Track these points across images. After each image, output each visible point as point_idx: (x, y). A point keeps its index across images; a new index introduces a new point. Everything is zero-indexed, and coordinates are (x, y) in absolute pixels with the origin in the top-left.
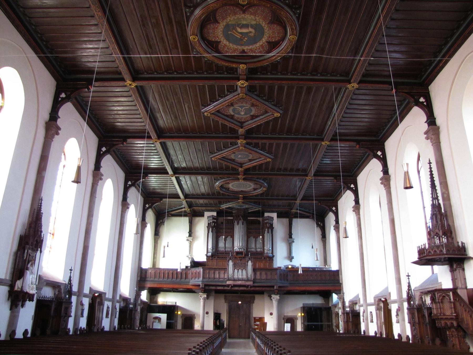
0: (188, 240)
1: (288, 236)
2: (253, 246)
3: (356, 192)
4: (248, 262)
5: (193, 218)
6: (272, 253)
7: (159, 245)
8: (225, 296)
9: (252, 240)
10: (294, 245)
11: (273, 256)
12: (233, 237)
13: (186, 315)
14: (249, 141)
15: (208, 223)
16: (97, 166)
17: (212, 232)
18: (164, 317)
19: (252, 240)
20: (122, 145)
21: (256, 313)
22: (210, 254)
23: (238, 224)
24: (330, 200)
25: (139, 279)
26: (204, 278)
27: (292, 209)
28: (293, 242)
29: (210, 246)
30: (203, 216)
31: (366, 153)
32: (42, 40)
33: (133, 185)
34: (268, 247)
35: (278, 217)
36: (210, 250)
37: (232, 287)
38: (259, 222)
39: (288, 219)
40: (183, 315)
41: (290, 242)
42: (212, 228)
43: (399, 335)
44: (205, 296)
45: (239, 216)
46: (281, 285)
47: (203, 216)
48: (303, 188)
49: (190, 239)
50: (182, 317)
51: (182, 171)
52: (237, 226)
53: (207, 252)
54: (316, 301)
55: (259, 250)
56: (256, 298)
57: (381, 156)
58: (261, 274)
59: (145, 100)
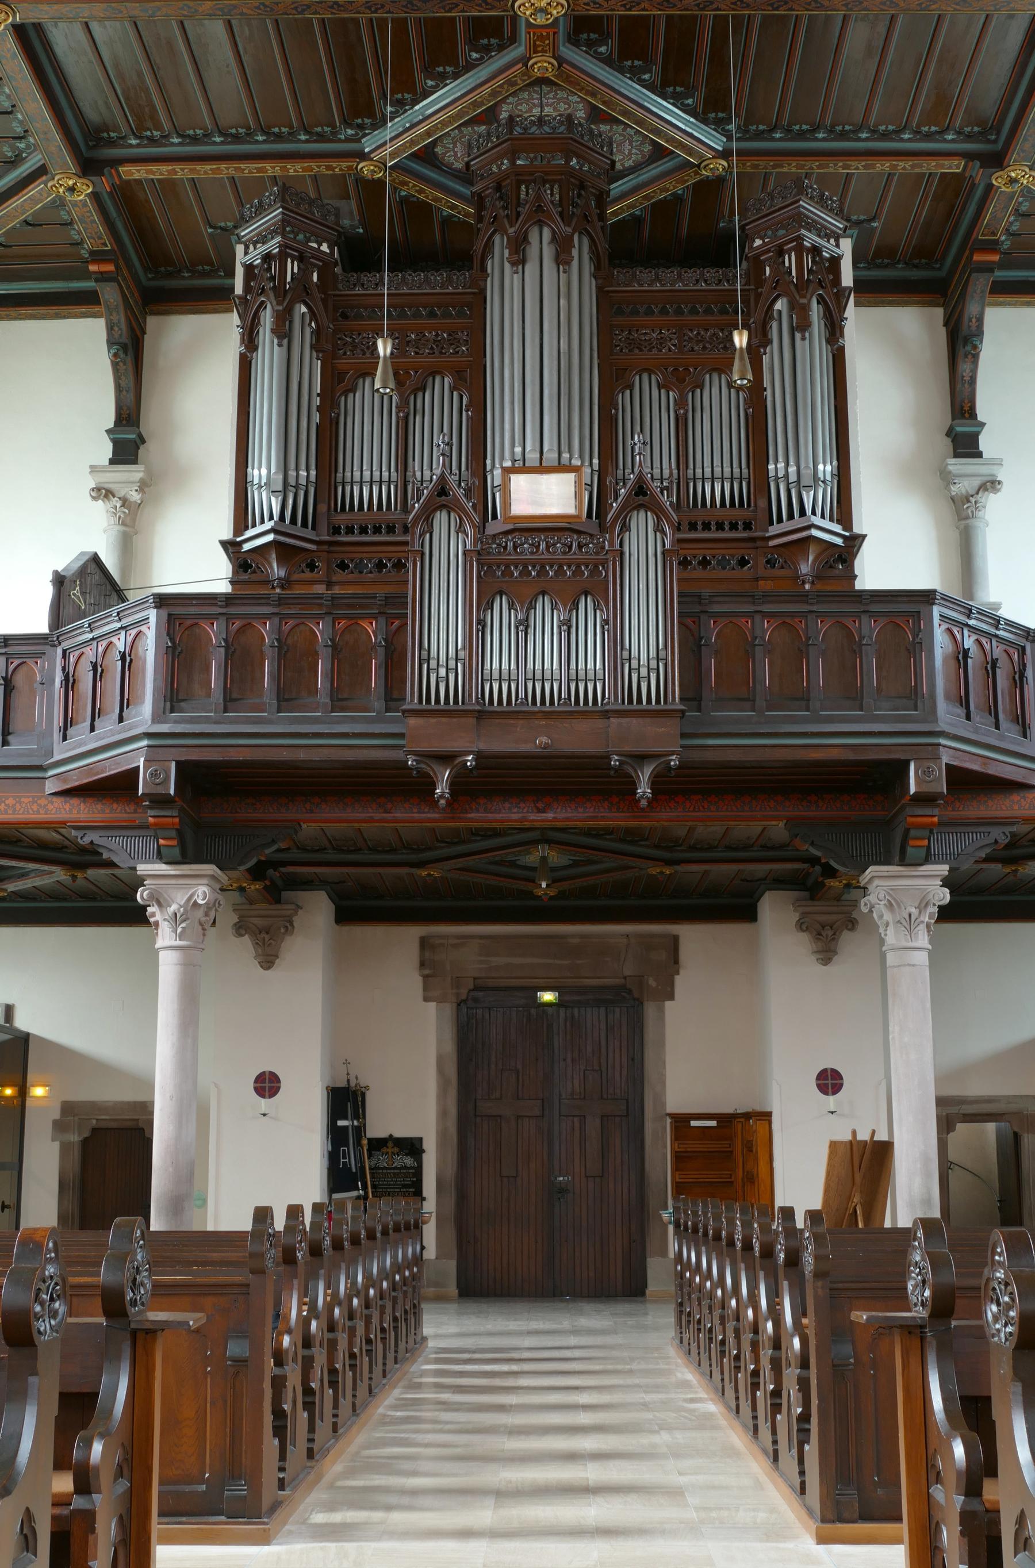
0: (103, 493)
1: (945, 444)
4: (625, 528)
5: (152, 322)
6: (843, 508)
9: (649, 402)
10: (994, 509)
11: (854, 542)
12: (472, 380)
17: (283, 331)
19: (649, 402)
22: (259, 536)
23: (519, 260)
26: (174, 696)
27: (997, 160)
28: (991, 485)
29: (263, 470)
34: (801, 466)
36: (267, 502)
37: (461, 787)
39: (939, 312)
41: (962, 487)
44: (202, 893)
46: (972, 759)
50: (59, 1127)
52: (512, 280)
53: (242, 516)
55: (716, 491)
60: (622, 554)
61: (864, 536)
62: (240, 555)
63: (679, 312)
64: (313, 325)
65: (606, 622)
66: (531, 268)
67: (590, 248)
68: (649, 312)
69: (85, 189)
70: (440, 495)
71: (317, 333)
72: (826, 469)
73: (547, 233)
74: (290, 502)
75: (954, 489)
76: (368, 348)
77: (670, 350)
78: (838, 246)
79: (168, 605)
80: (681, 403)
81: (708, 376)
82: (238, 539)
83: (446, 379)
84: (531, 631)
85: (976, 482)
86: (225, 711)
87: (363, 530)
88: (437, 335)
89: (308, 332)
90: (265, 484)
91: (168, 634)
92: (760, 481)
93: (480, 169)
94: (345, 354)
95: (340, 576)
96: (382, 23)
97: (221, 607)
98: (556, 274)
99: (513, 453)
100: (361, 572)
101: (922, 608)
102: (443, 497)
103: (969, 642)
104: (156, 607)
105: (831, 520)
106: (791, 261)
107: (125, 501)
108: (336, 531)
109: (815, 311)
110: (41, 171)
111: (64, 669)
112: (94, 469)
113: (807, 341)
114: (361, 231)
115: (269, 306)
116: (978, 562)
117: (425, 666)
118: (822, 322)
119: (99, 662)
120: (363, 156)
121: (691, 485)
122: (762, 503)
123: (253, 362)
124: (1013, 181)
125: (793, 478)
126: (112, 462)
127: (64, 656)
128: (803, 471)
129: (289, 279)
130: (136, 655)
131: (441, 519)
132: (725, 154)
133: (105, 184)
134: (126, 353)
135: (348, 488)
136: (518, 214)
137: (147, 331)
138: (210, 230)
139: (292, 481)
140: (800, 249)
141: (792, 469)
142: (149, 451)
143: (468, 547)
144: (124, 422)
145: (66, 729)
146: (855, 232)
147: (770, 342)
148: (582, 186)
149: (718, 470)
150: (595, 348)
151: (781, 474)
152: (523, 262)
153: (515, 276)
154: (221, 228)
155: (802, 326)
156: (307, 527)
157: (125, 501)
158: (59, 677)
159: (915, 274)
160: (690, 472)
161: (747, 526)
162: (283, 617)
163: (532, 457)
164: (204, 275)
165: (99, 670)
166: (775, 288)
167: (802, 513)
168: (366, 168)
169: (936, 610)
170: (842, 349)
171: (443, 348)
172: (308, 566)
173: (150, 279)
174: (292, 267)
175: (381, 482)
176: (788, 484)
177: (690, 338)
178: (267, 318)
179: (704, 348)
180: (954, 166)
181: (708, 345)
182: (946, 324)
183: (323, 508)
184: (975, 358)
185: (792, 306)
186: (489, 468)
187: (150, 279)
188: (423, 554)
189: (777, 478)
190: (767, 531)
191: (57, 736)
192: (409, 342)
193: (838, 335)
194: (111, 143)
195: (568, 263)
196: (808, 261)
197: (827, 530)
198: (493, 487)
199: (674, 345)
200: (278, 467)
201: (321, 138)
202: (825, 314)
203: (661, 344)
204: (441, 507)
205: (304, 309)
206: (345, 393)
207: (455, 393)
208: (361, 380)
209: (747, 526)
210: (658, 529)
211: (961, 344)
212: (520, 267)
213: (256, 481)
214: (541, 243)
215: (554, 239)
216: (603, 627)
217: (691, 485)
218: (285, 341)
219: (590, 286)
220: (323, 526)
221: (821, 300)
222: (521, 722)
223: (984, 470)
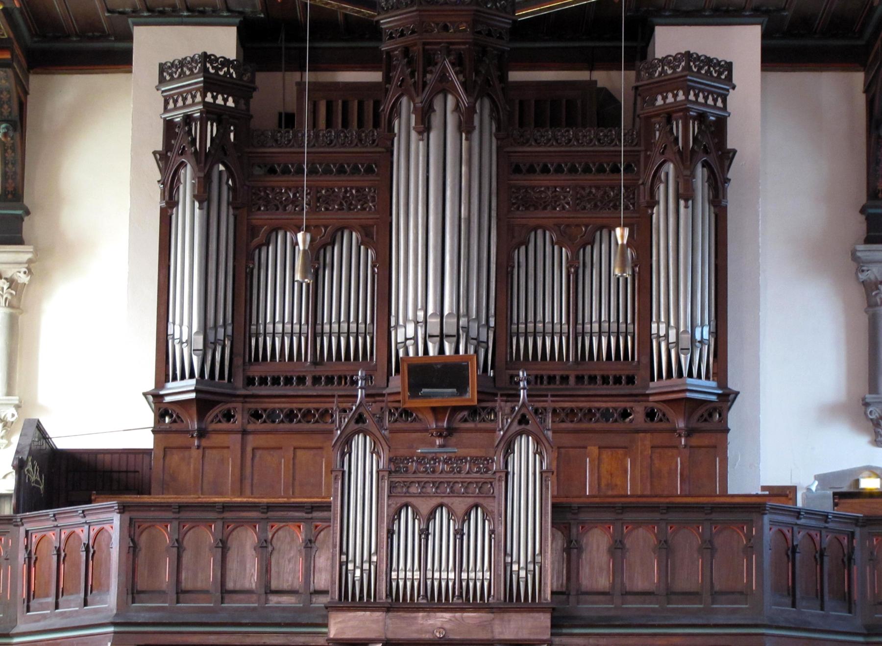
2: (554, 311)
4: (509, 449)
5: (35, 81)
6: (719, 367)
12: (379, 237)
15: (169, 125)
17: (202, 196)
22: (182, 389)
30: (118, 59)
35: (773, 58)
38: (604, 110)
42: (205, 161)
45: (430, 61)
47: (118, 59)
52: (417, 146)
53: (165, 370)
58: (617, 548)
60: (507, 474)
61: (737, 393)
62: (161, 405)
63: (573, 170)
64: (230, 182)
65: (492, 532)
67: (492, 111)
68: (545, 170)
70: (357, 422)
71: (233, 190)
74: (209, 358)
76: (281, 202)
77: (564, 208)
78: (725, 108)
79: (129, 511)
81: (598, 233)
82: (162, 392)
83: (354, 234)
84: (430, 537)
86: (178, 602)
87: (276, 381)
88: (346, 192)
89: (225, 189)
90: (187, 342)
91: (130, 536)
92: (646, 338)
93: (386, 29)
94: (259, 209)
97: (174, 513)
98: (458, 142)
99: (415, 315)
100: (274, 422)
101: (754, 516)
102: (360, 425)
104: (119, 513)
105: (707, 378)
106: (678, 128)
111: (26, 547)
113: (690, 209)
114: (262, 16)
115: (189, 166)
117: (344, 567)
118: (706, 184)
119: (62, 546)
121: (580, 339)
122: (645, 360)
123: (174, 217)
125: (672, 338)
127: (27, 536)
128: (682, 336)
129: (208, 145)
130: (100, 546)
134: (15, 130)
135: (261, 340)
136: (425, 84)
137: (30, 92)
138: (107, 14)
139: (211, 338)
141: (672, 333)
143: (381, 467)
144: (10, 196)
145: (29, 601)
146: (765, 19)
147: (658, 203)
149: (605, 326)
150: (494, 214)
151: (662, 333)
153: (421, 143)
154: (120, 13)
156: (224, 379)
158: (22, 555)
160: (580, 327)
165: (63, 554)
166: (663, 153)
167: (680, 374)
170: (725, 209)
171: (351, 204)
172: (224, 416)
173: (36, 42)
174: (212, 129)
175: (292, 334)
176: (668, 344)
177: (582, 196)
178: (188, 177)
179: (596, 206)
181: (599, 203)
182: (867, 91)
183: (238, 361)
186: (393, 323)
187: (36, 42)
188: (343, 472)
189: (659, 336)
190: (648, 387)
191: (21, 607)
192: (320, 197)
193: (721, 196)
195: (469, 133)
196: (694, 128)
198: (397, 343)
199: (568, 203)
200: (199, 327)
202: (709, 178)
203: (556, 202)
204: (358, 432)
205: (221, 168)
206: (259, 247)
207: (362, 247)
208: (274, 234)
209: (631, 380)
212: (425, 134)
213: (177, 336)
215: (457, 108)
216: (490, 536)
217: (580, 339)
218: (205, 204)
219: (491, 145)
221: (705, 164)
222: (421, 614)
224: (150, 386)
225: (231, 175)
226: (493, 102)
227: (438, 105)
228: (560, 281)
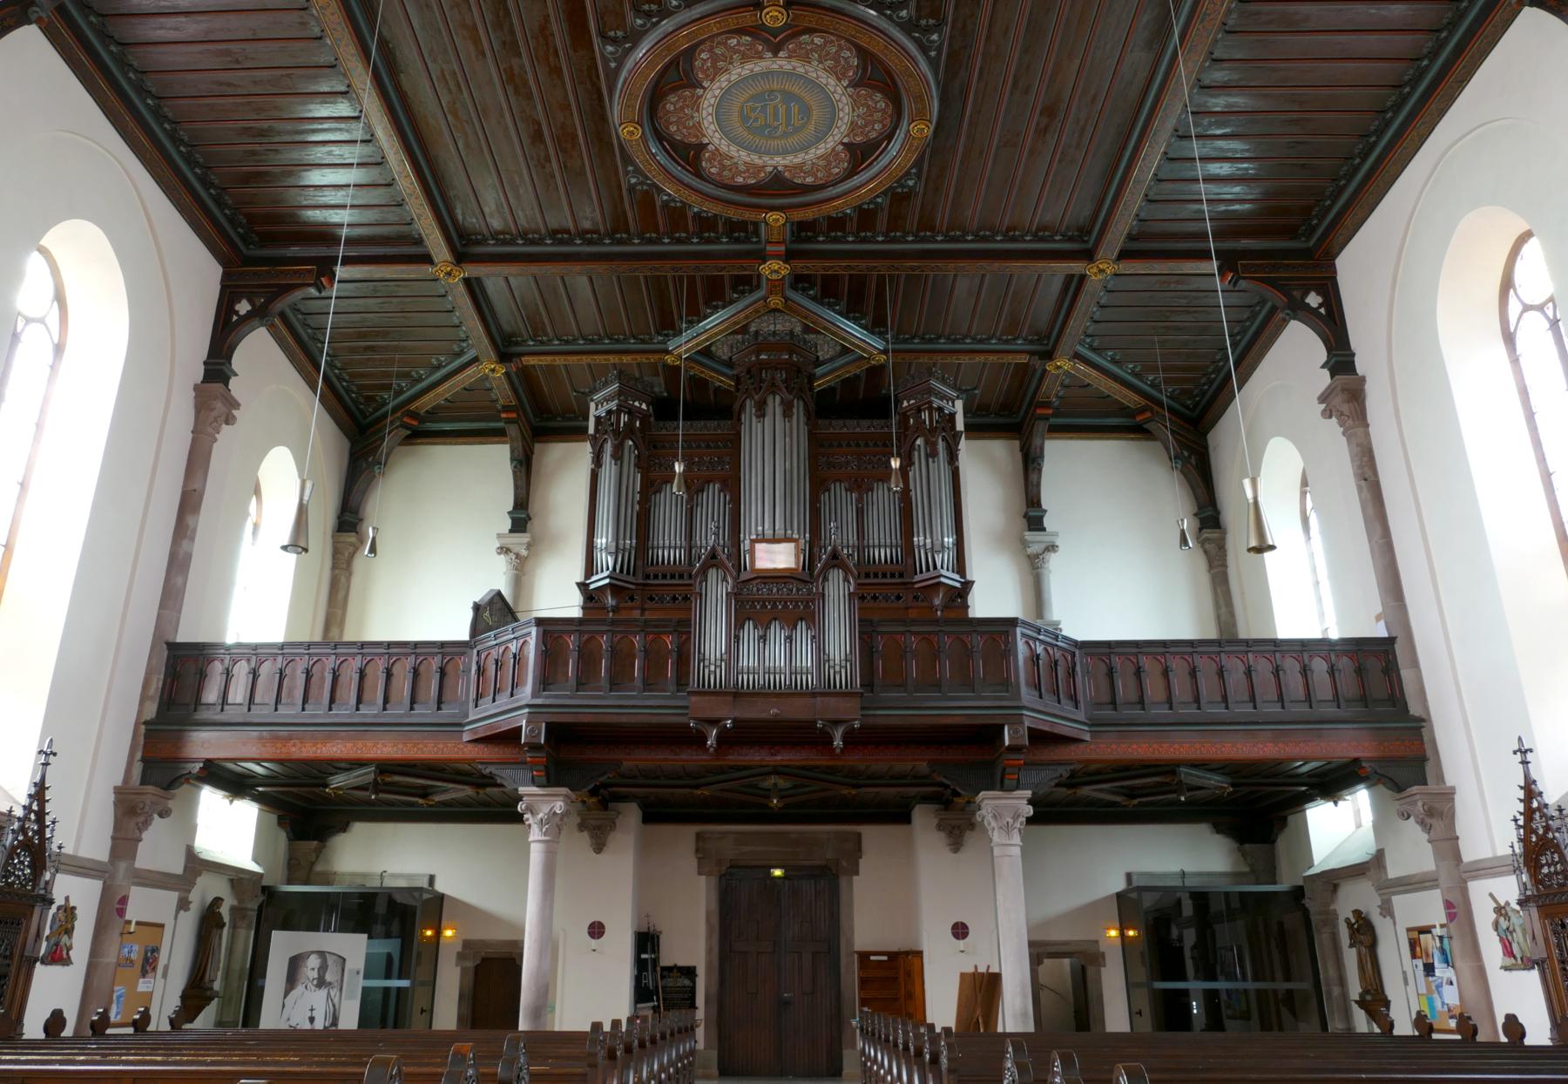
0: (504, 550)
3: (1333, 329)
4: (826, 579)
5: (537, 447)
6: (960, 566)
7: (356, 580)
8: (699, 837)
9: (841, 501)
10: (1054, 563)
11: (967, 585)
12: (732, 486)
13: (483, 943)
14: (802, 266)
16: (217, 369)
17: (617, 456)
18: (354, 948)
19: (841, 501)
20: (313, 291)
21: (868, 927)
22: (600, 580)
23: (761, 415)
24: (1286, 254)
25: (151, 711)
26: (545, 681)
27: (1048, 355)
28: (1052, 548)
31: (1263, 302)
32: (142, 91)
33: (259, 314)
34: (933, 540)
36: (605, 560)
37: (725, 740)
39: (1017, 443)
40: (468, 947)
43: (1421, 1021)
44: (559, 806)
46: (1045, 723)
48: (1109, 237)
49: (519, 541)
50: (461, 957)
51: (492, 248)
52: (757, 426)
53: (590, 569)
54: (1188, 856)
55: (881, 554)
56: (866, 844)
57: (1322, 311)
59: (412, 138)
63: (858, 445)
65: (813, 637)
66: (768, 420)
68: (840, 445)
69: (501, 371)
71: (638, 457)
72: (949, 540)
73: (778, 398)
75: (1029, 551)
80: (860, 500)
85: (1043, 546)
92: (909, 548)
95: (649, 604)
96: (681, 278)
103: (1040, 649)
106: (925, 416)
107: (517, 556)
108: (648, 577)
109: (941, 446)
110: (475, 360)
112: (499, 536)
116: (1045, 595)
120: (667, 352)
122: (910, 561)
124: (1059, 367)
126: (511, 531)
131: (712, 573)
132: (885, 352)
133: (513, 367)
140: (931, 409)
142: (534, 525)
148: (799, 371)
152: (764, 416)
155: (932, 454)
157: (517, 556)
158: (474, 668)
159: (1001, 420)
161: (901, 575)
162: (614, 633)
163: (769, 533)
164: (570, 419)
167: (935, 567)
168: (669, 359)
169: (1019, 630)
170: (957, 469)
174: (624, 418)
178: (608, 448)
180: (1024, 359)
184: (1040, 471)
185: (927, 442)
191: (471, 704)
194: (517, 344)
196: (936, 416)
197: (951, 578)
201: (643, 341)
210: (846, 580)
211: (1031, 463)
214: (774, 404)
215: (782, 402)
219: (804, 430)
220: (640, 574)
223: (1047, 539)
224: (580, 578)
225: (636, 447)
226: (806, 404)
227: (770, 400)
228: (850, 515)
